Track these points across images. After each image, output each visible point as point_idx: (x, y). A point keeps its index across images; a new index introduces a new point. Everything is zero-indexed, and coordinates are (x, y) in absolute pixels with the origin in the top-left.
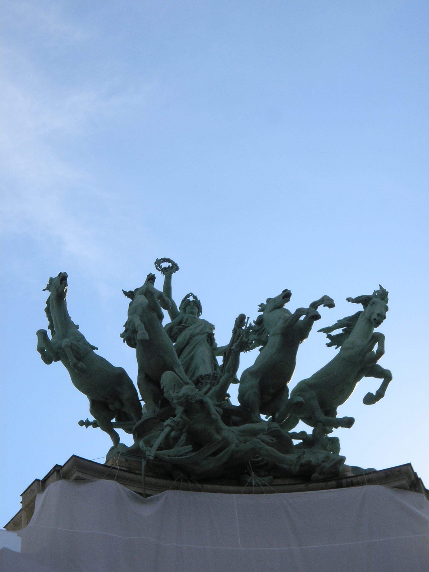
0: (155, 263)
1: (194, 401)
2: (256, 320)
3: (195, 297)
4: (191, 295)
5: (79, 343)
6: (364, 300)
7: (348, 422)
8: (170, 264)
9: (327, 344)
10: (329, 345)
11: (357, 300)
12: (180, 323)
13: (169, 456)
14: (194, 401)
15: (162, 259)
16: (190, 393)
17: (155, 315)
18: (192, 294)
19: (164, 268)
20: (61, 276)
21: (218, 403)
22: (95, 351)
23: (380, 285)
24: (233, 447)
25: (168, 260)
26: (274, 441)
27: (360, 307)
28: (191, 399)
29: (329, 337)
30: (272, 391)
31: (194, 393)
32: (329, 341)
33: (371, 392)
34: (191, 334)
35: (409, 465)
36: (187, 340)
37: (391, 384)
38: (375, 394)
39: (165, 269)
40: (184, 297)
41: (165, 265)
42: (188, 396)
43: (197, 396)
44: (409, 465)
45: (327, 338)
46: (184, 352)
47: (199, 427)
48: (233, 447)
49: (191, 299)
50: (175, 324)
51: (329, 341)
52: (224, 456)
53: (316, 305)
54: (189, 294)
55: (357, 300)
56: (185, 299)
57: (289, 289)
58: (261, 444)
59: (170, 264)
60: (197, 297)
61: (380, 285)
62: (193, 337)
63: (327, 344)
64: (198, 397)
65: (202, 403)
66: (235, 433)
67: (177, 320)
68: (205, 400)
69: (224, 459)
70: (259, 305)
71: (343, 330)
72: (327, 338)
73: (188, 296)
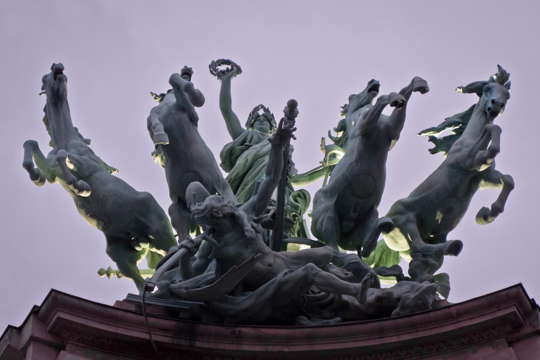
0: (210, 67)
1: (221, 215)
2: (336, 127)
3: (267, 110)
4: (261, 108)
5: (83, 157)
6: (477, 88)
7: (456, 248)
8: (229, 67)
9: (430, 150)
10: (433, 151)
11: (469, 89)
12: (244, 141)
13: (186, 289)
14: (221, 215)
15: (219, 61)
16: (215, 204)
17: (185, 117)
18: (263, 107)
19: (221, 71)
20: (54, 67)
21: (256, 218)
22: (114, 174)
23: (498, 66)
24: (280, 277)
25: (227, 62)
26: (349, 275)
27: (474, 99)
29: (432, 139)
30: (353, 215)
31: (220, 204)
32: (433, 146)
33: (486, 207)
34: (256, 155)
35: (520, 285)
37: (512, 194)
38: (490, 209)
39: (223, 72)
41: (223, 68)
42: (213, 208)
43: (226, 207)
44: (520, 285)
45: (429, 141)
46: (246, 178)
47: (231, 250)
48: (280, 277)
49: (261, 112)
50: (236, 144)
51: (433, 146)
52: (267, 289)
53: (407, 92)
55: (469, 89)
57: (376, 80)
58: (316, 270)
60: (270, 109)
61: (498, 66)
62: (257, 159)
63: (430, 150)
64: (227, 210)
66: (283, 259)
67: (240, 139)
68: (237, 213)
69: (269, 293)
70: (343, 108)
71: (454, 131)
72: (429, 141)
73: (257, 109)
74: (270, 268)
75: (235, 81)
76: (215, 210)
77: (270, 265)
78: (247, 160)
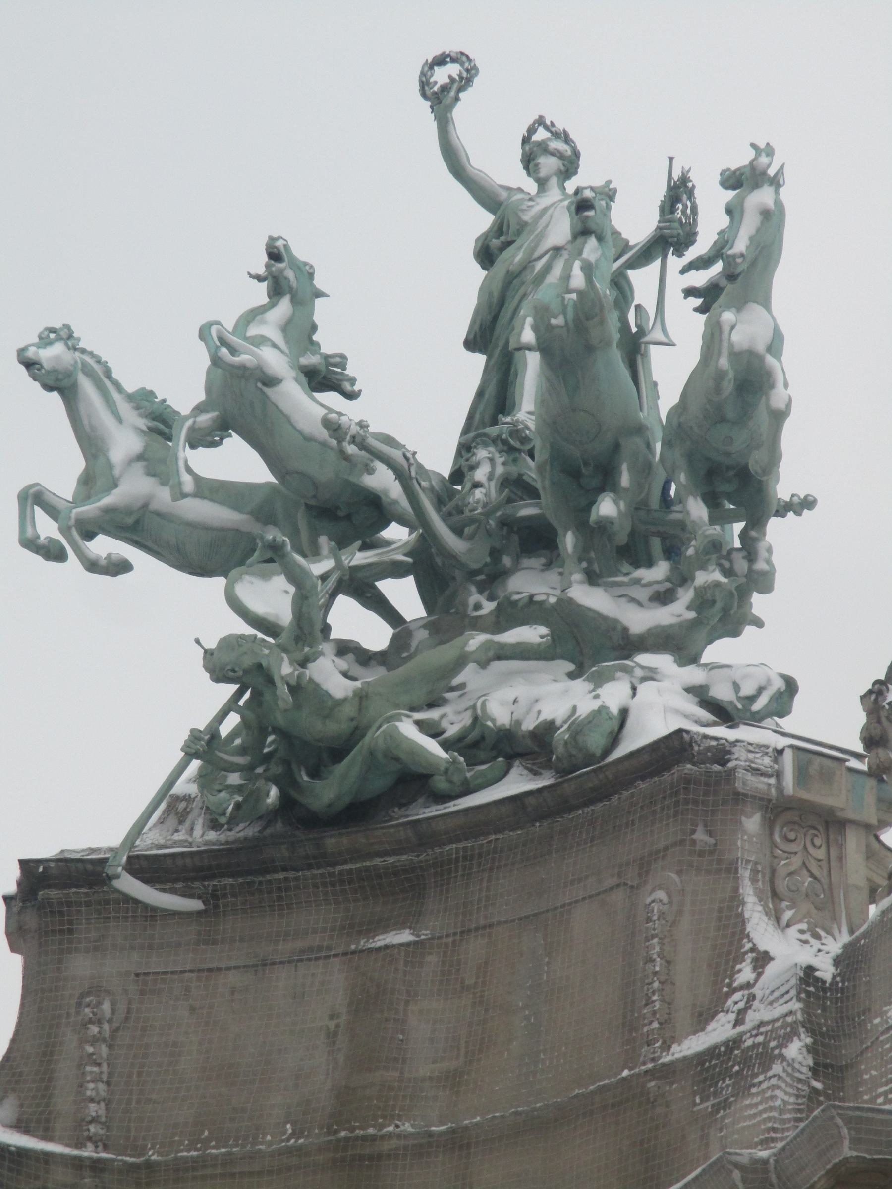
4: (540, 125)
8: (453, 69)
9: (696, 310)
12: (499, 229)
14: (241, 673)
18: (540, 121)
28: (234, 671)
32: (698, 302)
36: (496, 294)
40: (524, 131)
41: (441, 76)
45: (685, 298)
49: (541, 135)
51: (698, 302)
54: (534, 123)
56: (525, 140)
59: (453, 69)
62: (510, 283)
63: (696, 310)
64: (247, 662)
65: (260, 666)
68: (264, 664)
72: (685, 298)
73: (532, 131)
74: (354, 723)
75: (459, 113)
76: (229, 667)
77: (352, 720)
78: (491, 294)
